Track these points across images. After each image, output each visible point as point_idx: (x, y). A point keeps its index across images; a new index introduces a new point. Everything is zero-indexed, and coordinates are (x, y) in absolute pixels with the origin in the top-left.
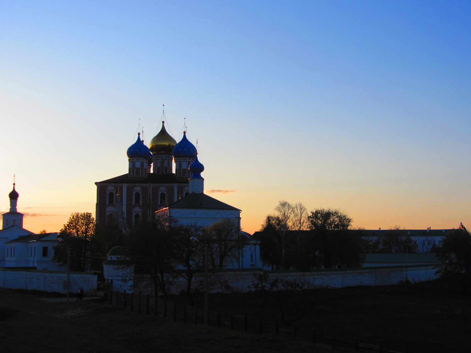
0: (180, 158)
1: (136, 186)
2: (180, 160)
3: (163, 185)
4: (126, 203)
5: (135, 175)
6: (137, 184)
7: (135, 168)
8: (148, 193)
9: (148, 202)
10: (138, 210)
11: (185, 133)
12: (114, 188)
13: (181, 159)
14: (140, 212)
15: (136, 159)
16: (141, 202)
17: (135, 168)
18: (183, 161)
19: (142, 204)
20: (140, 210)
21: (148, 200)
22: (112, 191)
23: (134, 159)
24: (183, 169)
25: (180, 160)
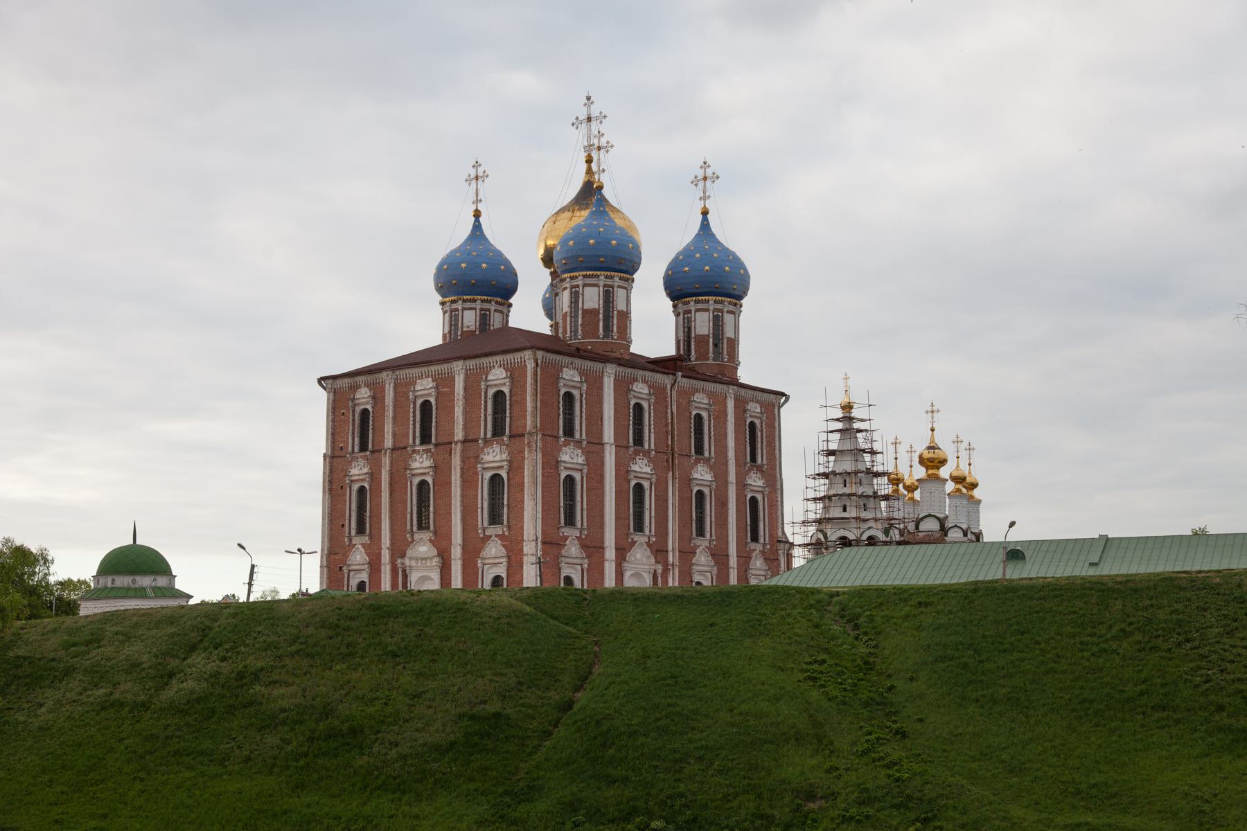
0: (723, 299)
1: (637, 381)
2: (719, 306)
3: (703, 389)
4: (612, 441)
5: (616, 337)
6: (641, 373)
7: (615, 312)
8: (669, 411)
9: (670, 442)
10: (641, 467)
11: (705, 213)
12: (577, 379)
13: (722, 302)
14: (648, 476)
15: (585, 276)
16: (650, 441)
17: (615, 312)
18: (729, 312)
19: (653, 446)
20: (647, 470)
21: (670, 437)
22: (573, 387)
23: (612, 277)
24: (729, 339)
25: (719, 306)
